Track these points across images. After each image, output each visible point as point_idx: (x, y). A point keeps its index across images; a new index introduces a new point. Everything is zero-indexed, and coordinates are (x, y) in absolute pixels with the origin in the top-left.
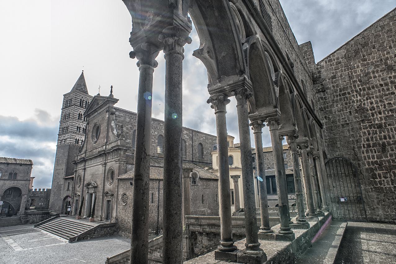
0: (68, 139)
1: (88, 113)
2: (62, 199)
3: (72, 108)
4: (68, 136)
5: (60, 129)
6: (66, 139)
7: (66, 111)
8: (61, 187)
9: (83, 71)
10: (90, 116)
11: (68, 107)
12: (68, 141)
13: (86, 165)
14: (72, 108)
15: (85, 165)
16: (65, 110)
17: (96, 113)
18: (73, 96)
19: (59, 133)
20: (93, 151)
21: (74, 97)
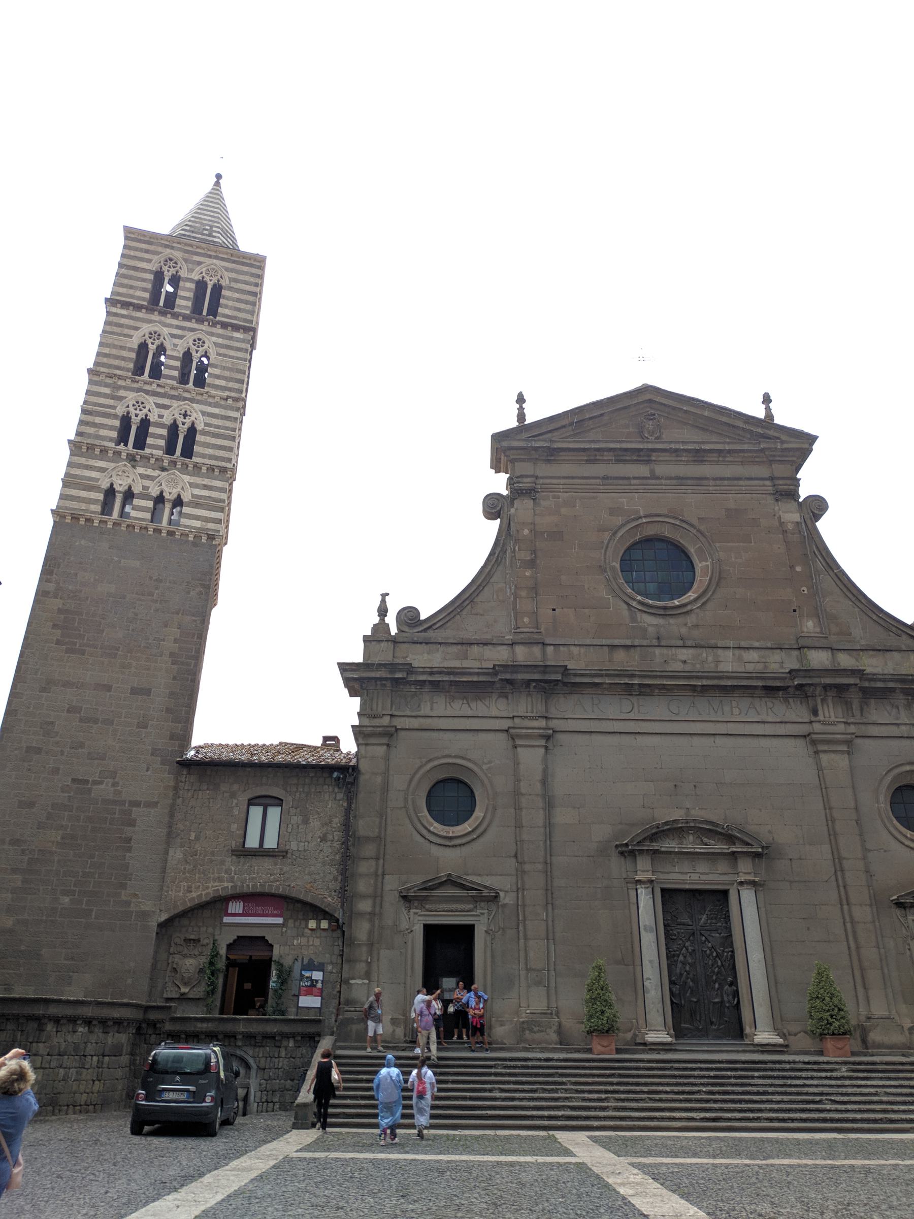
0: (196, 505)
1: (555, 446)
2: (144, 915)
3: (219, 336)
4: (197, 492)
5: (84, 411)
6: (178, 502)
7: (166, 331)
8: (132, 823)
9: (219, 176)
10: (548, 461)
11: (186, 318)
12: (197, 518)
13: (553, 712)
14: (231, 338)
15: (547, 711)
16: (150, 321)
17: (643, 470)
18: (232, 280)
19: (79, 434)
20: (657, 651)
21: (233, 285)
